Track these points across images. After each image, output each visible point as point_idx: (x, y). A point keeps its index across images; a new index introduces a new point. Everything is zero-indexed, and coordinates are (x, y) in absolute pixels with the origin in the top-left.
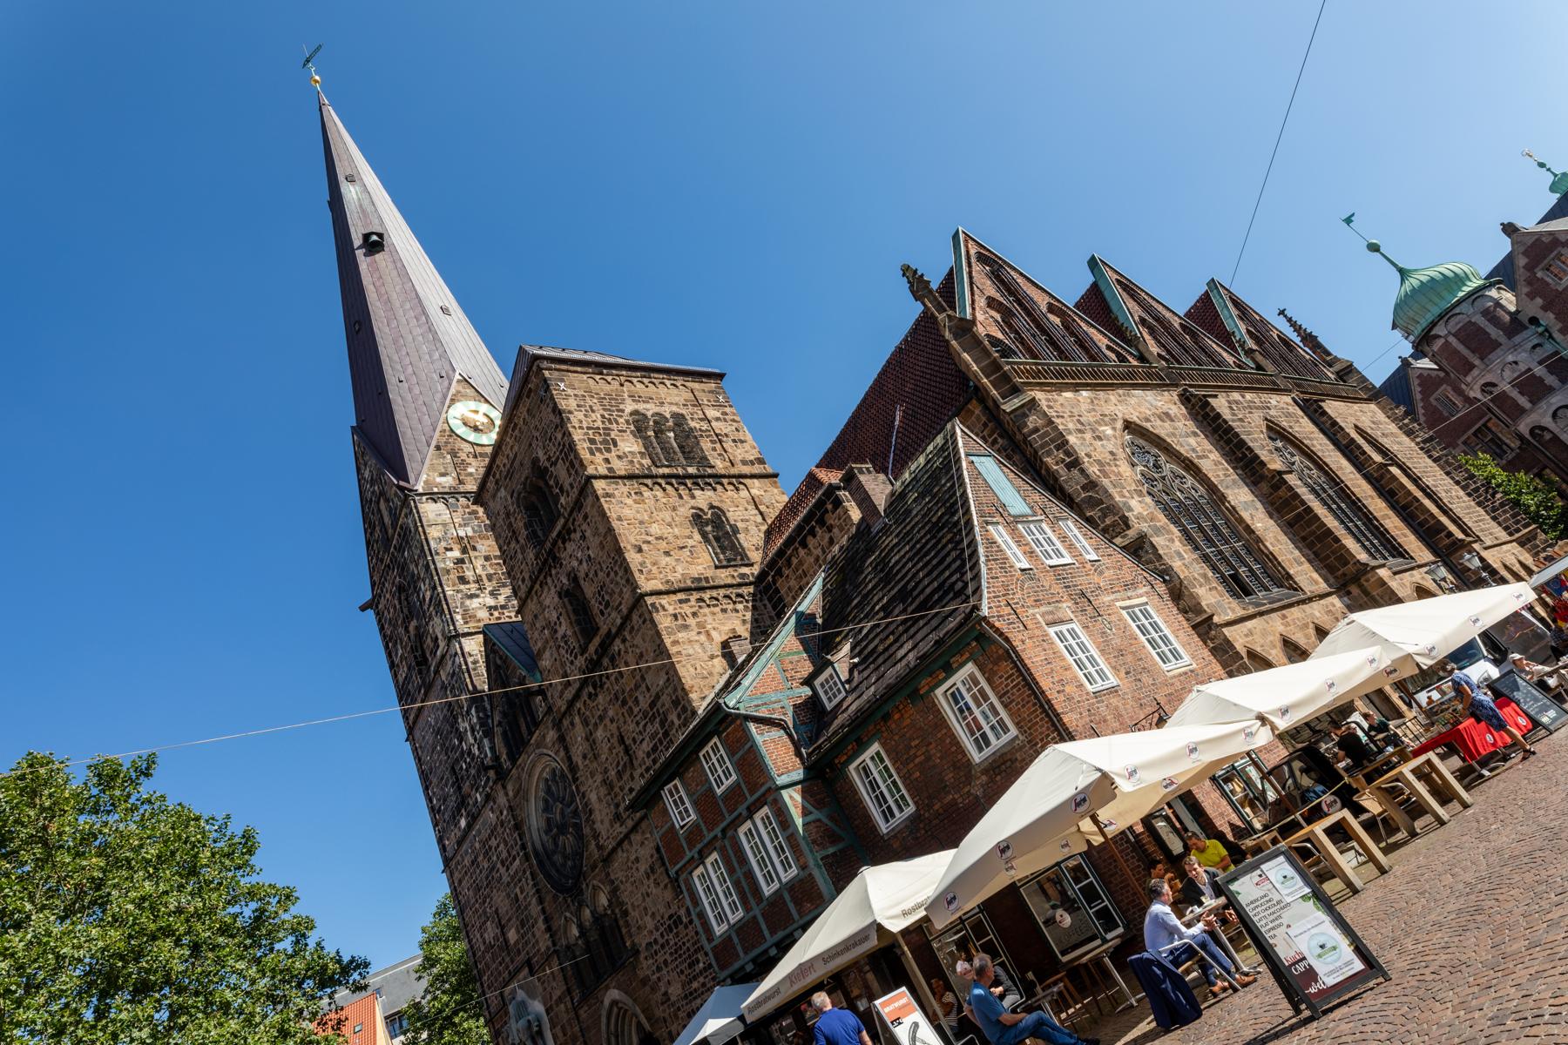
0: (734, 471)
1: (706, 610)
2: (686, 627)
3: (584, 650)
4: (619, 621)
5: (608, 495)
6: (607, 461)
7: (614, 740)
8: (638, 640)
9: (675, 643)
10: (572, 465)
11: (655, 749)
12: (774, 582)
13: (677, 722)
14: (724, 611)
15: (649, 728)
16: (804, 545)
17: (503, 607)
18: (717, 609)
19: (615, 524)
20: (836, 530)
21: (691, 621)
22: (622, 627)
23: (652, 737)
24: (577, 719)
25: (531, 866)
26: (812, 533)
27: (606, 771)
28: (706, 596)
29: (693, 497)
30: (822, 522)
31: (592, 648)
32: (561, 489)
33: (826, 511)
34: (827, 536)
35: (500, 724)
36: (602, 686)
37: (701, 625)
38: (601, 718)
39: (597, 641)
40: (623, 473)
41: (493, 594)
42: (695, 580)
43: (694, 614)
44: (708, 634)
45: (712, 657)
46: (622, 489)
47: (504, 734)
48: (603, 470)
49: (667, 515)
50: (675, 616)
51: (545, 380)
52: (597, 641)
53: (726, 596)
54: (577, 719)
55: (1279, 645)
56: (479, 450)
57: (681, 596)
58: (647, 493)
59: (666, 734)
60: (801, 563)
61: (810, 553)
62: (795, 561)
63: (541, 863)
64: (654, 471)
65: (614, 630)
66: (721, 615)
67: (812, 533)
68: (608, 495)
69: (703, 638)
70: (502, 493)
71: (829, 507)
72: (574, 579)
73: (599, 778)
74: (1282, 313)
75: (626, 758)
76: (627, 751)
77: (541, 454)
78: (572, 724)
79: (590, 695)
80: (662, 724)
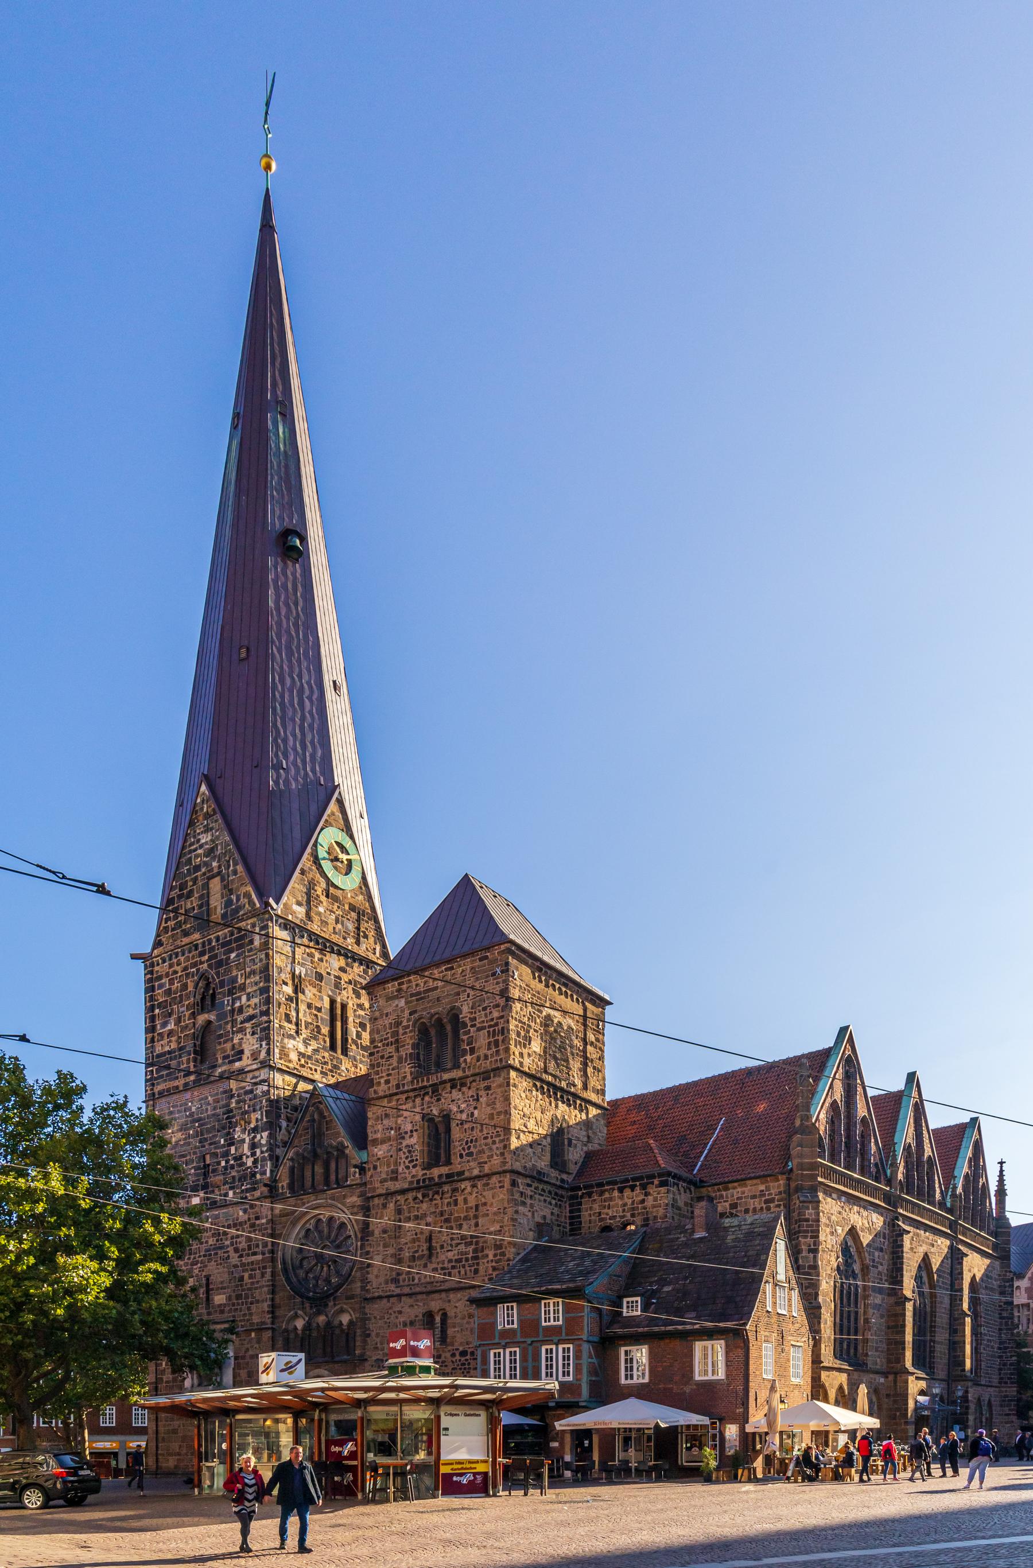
0: (585, 1095)
1: (537, 1196)
2: (524, 1204)
3: (428, 1166)
4: (476, 1172)
5: (515, 1086)
6: (521, 1055)
7: (423, 1238)
8: (488, 1194)
9: (517, 1212)
10: (496, 1043)
11: (459, 1261)
12: (582, 1197)
13: (491, 1257)
14: (545, 1201)
15: (462, 1247)
16: (621, 1190)
17: (310, 1058)
18: (542, 1198)
19: (513, 1111)
20: (650, 1198)
21: (528, 1201)
22: (478, 1177)
23: (462, 1253)
24: (392, 1205)
25: (274, 1267)
26: (633, 1188)
27: (401, 1249)
28: (541, 1187)
29: (557, 1107)
30: (644, 1187)
31: (436, 1172)
32: (472, 1051)
33: (653, 1183)
34: (642, 1197)
35: (292, 1159)
36: (431, 1200)
37: (532, 1206)
38: (417, 1217)
39: (444, 1170)
40: (526, 1069)
41: (306, 1043)
42: (539, 1173)
43: (531, 1197)
44: (533, 1214)
45: (531, 1230)
46: (524, 1083)
47: (292, 1170)
48: (517, 1064)
49: (539, 1115)
50: (522, 1193)
51: (507, 964)
52: (444, 1170)
53: (550, 1192)
54: (392, 1205)
55: (837, 1387)
56: (332, 890)
57: (528, 1181)
58: (534, 1093)
59: (476, 1258)
60: (611, 1199)
61: (622, 1198)
62: (607, 1195)
63: (285, 1270)
64: (544, 1076)
65: (467, 1174)
66: (542, 1204)
67: (633, 1188)
68: (515, 1086)
69: (530, 1214)
70: (402, 1003)
71: (656, 1182)
72: (447, 1118)
73: (391, 1251)
74: (1001, 1163)
75: (426, 1252)
76: (430, 1248)
77: (465, 1009)
78: (385, 1206)
79: (415, 1198)
80: (475, 1251)
